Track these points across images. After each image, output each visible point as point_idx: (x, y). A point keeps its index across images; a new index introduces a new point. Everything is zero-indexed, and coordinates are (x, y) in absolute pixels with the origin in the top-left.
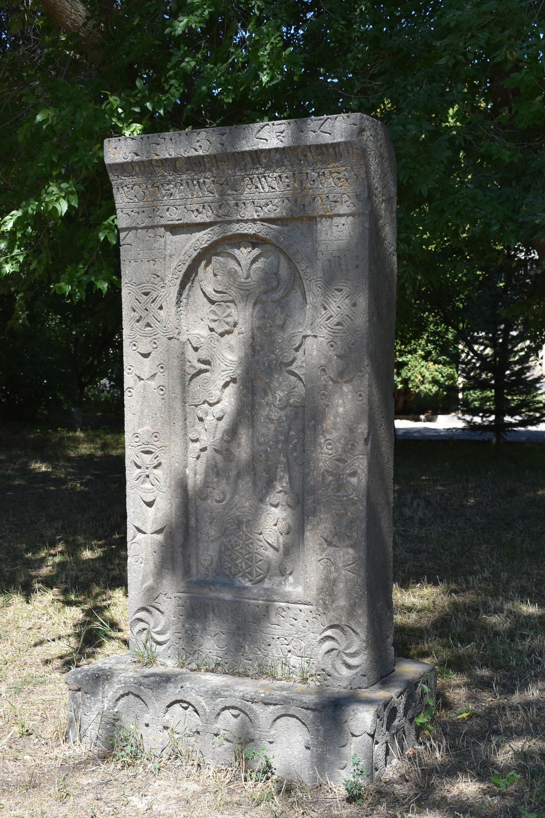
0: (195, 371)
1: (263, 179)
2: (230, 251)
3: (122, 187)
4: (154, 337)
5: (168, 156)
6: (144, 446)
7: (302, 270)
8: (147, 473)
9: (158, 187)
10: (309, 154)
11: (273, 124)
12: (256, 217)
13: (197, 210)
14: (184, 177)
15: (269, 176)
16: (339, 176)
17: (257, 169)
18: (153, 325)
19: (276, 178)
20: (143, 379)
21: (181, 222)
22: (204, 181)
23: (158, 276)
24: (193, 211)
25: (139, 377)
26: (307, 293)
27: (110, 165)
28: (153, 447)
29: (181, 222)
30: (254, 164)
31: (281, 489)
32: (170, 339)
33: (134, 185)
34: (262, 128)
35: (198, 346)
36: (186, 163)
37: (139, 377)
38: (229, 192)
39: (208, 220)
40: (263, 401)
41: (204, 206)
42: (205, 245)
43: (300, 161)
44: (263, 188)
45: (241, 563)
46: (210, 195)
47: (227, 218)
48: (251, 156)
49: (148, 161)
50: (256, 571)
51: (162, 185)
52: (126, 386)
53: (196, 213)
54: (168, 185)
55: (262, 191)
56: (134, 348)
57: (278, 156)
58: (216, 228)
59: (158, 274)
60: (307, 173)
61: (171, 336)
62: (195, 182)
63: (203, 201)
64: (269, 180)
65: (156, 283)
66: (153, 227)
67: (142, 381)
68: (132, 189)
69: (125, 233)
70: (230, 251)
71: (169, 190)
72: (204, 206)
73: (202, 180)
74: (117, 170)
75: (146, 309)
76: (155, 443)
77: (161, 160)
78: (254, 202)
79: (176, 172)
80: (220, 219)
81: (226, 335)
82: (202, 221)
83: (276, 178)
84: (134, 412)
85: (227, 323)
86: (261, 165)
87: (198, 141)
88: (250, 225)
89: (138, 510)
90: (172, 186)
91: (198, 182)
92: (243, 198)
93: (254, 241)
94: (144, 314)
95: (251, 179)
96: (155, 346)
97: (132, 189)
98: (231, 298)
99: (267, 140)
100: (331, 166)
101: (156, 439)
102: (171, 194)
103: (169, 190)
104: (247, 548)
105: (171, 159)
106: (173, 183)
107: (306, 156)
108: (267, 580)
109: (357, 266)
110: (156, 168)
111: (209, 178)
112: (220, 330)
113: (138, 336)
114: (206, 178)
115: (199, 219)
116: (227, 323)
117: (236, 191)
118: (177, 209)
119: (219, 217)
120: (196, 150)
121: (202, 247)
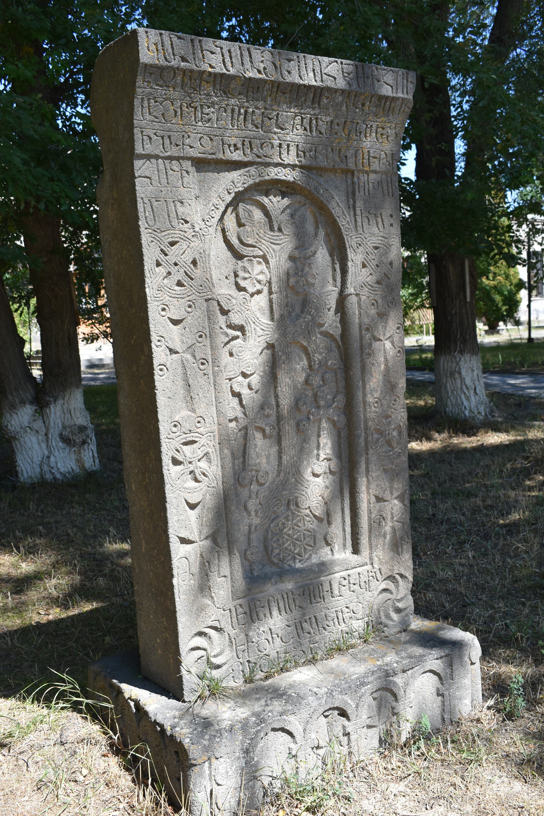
0: (227, 339)
1: (314, 122)
2: (258, 198)
3: (149, 99)
4: (188, 298)
5: (224, 71)
6: (184, 436)
7: (343, 225)
8: (192, 469)
9: (196, 108)
10: (368, 103)
11: (342, 63)
12: (297, 163)
13: (235, 145)
14: (232, 101)
15: (321, 119)
16: (383, 132)
17: (314, 109)
18: (185, 284)
19: (327, 122)
20: (177, 353)
21: (214, 156)
22: (253, 112)
23: (186, 222)
24: (229, 146)
25: (171, 350)
26: (348, 250)
27: (146, 65)
28: (197, 435)
29: (214, 156)
30: (313, 102)
31: (325, 456)
32: (207, 300)
33: (166, 99)
34: (330, 64)
35: (230, 309)
36: (242, 85)
37: (171, 350)
38: (275, 129)
39: (246, 159)
40: (298, 366)
41: (244, 141)
42: (241, 189)
43: (356, 108)
44: (311, 131)
45: (289, 545)
46: (254, 129)
47: (268, 160)
48: (314, 94)
49: (199, 72)
50: (305, 548)
51: (201, 106)
52: (156, 362)
53: (232, 149)
54: (209, 107)
55: (309, 134)
56: (163, 313)
57: (340, 99)
58: (252, 170)
59: (188, 219)
60: (358, 123)
61: (209, 297)
62: (242, 111)
63: (244, 136)
64: (321, 123)
65: (186, 230)
66: (178, 159)
67: (174, 356)
68: (161, 104)
69: (142, 162)
70: (258, 198)
71: (208, 114)
72: (244, 141)
73: (251, 110)
74: (151, 74)
75: (176, 264)
76: (198, 430)
77: (215, 75)
78: (298, 145)
79: (225, 93)
80: (259, 160)
81: (256, 295)
82: (240, 159)
83: (327, 122)
84: (170, 395)
85: (259, 282)
86: (319, 105)
87: (262, 62)
88: (287, 170)
89: (182, 517)
90: (212, 110)
91: (246, 112)
92: (289, 139)
93: (284, 189)
94: (174, 269)
95: (302, 119)
96: (189, 310)
97: (161, 104)
98: (261, 253)
99: (335, 78)
100: (380, 120)
101: (199, 425)
102: (209, 120)
103: (208, 114)
104: (296, 527)
105: (229, 75)
106: (216, 107)
107: (363, 105)
108: (313, 556)
109: (391, 225)
110: (203, 83)
111: (260, 109)
112: (251, 290)
113: (168, 298)
114: (257, 108)
115: (237, 156)
116: (259, 282)
117: (282, 129)
118: (211, 140)
119: (259, 157)
120: (259, 72)
121: (237, 190)
